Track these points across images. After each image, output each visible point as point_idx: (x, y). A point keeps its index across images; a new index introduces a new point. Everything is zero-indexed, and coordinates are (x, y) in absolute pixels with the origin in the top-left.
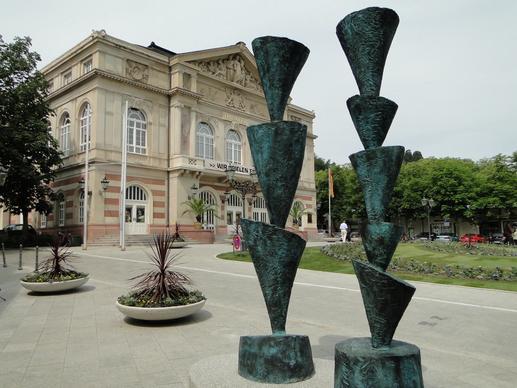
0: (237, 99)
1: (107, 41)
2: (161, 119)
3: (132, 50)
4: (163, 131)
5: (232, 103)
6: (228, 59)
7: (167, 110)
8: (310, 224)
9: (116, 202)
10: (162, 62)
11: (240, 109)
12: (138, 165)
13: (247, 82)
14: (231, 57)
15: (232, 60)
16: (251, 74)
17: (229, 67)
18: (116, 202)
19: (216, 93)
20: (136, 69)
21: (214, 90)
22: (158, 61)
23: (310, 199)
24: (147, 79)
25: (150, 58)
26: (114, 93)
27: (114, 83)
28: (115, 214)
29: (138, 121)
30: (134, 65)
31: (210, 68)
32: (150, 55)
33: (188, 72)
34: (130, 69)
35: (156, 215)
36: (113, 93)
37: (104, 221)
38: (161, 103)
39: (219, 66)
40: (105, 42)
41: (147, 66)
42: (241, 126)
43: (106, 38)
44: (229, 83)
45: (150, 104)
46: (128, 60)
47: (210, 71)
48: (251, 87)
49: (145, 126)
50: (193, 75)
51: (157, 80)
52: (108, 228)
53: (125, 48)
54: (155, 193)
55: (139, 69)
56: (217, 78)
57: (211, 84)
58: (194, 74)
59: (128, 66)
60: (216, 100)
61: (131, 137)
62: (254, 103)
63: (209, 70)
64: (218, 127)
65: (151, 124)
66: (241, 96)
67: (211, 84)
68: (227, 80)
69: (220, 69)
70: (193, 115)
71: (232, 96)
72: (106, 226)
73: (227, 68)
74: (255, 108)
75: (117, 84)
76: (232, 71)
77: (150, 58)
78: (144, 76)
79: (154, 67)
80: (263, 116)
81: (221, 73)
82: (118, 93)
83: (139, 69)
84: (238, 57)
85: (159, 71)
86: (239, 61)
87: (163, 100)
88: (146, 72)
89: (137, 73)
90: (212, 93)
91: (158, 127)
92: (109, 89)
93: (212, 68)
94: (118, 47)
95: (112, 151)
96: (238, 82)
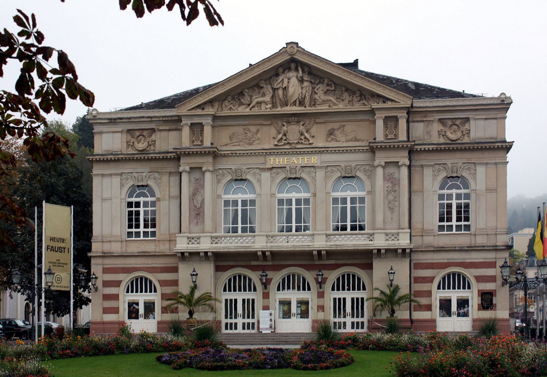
0: (293, 131)
1: (100, 119)
2: (171, 190)
3: (130, 118)
4: (175, 204)
5: (284, 138)
6: (277, 75)
7: (178, 178)
8: (487, 314)
9: (116, 297)
10: (170, 119)
11: (302, 143)
12: (138, 252)
13: (316, 96)
14: (281, 70)
15: (283, 72)
16: (325, 82)
17: (275, 87)
18: (116, 297)
19: (258, 131)
20: (141, 137)
21: (253, 129)
22: (164, 119)
23: (492, 265)
24: (154, 145)
25: (153, 119)
26: (111, 175)
27: (112, 165)
28: (116, 311)
29: (146, 199)
30: (138, 133)
31: (242, 100)
32: (150, 115)
33: (196, 120)
34: (132, 140)
35: (165, 310)
36: (111, 175)
37: (102, 319)
38: (172, 171)
39: (262, 91)
40: (98, 121)
41: (153, 129)
42: (307, 169)
43: (98, 117)
44: (280, 110)
45: (157, 175)
46: (129, 131)
47: (243, 104)
48: (324, 102)
49: (153, 204)
50: (204, 122)
51: (166, 142)
52: (106, 326)
53: (121, 119)
54: (163, 283)
55: (144, 136)
56: (256, 111)
57: (246, 122)
58: (207, 122)
59: (130, 138)
60: (257, 142)
61: (138, 220)
62: (336, 126)
63: (242, 104)
64: (259, 181)
65: (158, 200)
66: (301, 123)
67: (246, 122)
68: (274, 105)
69: (264, 95)
70: (208, 176)
71: (285, 128)
72: (104, 323)
73: (274, 90)
74: (337, 133)
75: (115, 164)
76: (280, 92)
77: (153, 119)
78: (150, 143)
79: (161, 128)
80: (356, 140)
81: (262, 102)
82: (116, 174)
83: (144, 136)
84: (293, 66)
85: (169, 130)
86: (297, 70)
87: (170, 167)
88: (153, 137)
89: (142, 141)
90: (249, 134)
91: (167, 202)
92: (104, 173)
93: (246, 100)
94: (113, 121)
95: (110, 242)
96: (294, 104)
